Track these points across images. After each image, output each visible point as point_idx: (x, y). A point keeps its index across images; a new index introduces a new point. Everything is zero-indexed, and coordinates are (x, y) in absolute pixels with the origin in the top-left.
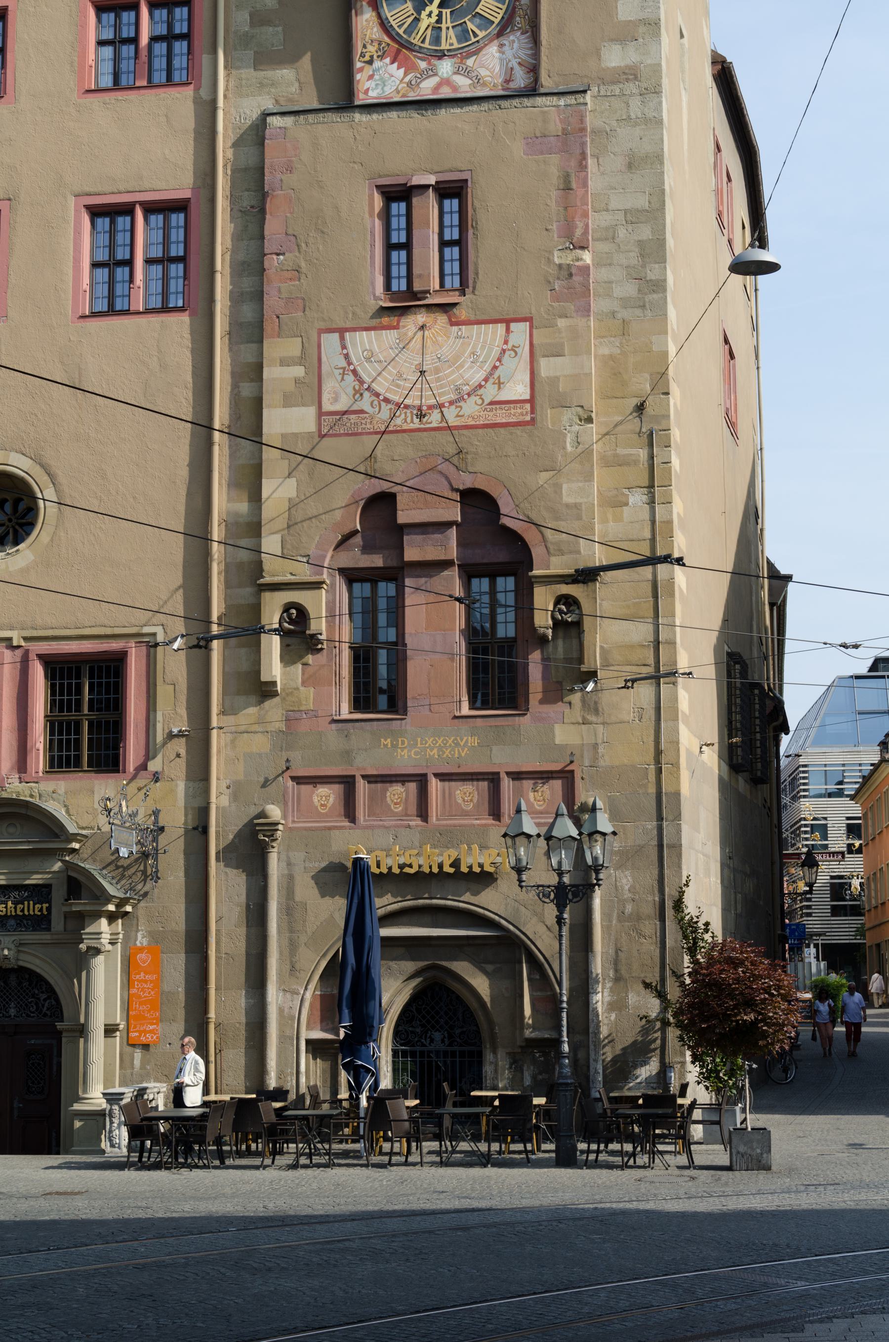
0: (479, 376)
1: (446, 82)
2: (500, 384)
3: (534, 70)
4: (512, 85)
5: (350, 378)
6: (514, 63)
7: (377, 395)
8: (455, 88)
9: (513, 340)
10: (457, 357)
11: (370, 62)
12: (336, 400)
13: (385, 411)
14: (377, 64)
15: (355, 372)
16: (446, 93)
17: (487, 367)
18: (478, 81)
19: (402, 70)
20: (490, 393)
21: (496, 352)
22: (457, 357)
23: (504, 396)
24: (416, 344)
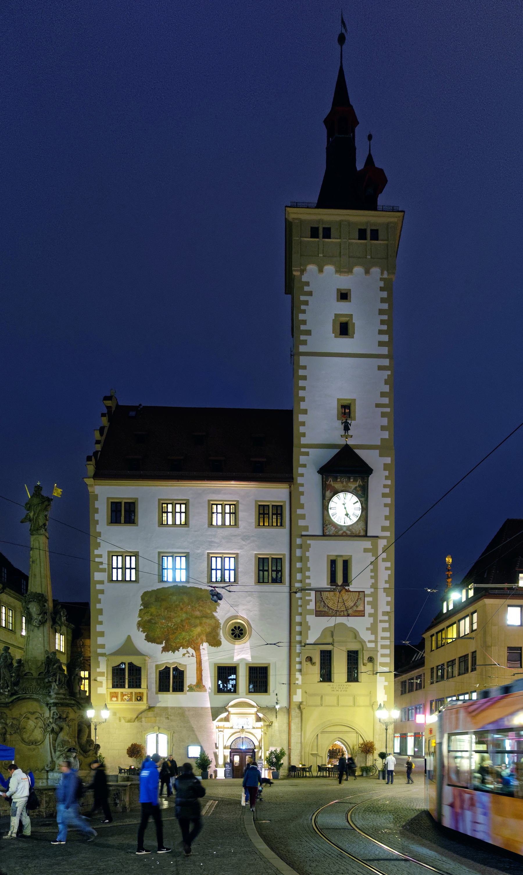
0: (353, 604)
1: (344, 532)
2: (357, 607)
3: (366, 531)
4: (360, 534)
5: (323, 603)
6: (361, 529)
7: (329, 607)
8: (346, 533)
9: (360, 596)
10: (347, 600)
11: (327, 525)
12: (319, 608)
13: (330, 612)
14: (328, 526)
15: (324, 602)
16: (345, 534)
17: (354, 602)
18: (352, 532)
19: (334, 529)
20: (355, 608)
21: (356, 598)
22: (347, 600)
23: (358, 609)
24: (337, 596)
